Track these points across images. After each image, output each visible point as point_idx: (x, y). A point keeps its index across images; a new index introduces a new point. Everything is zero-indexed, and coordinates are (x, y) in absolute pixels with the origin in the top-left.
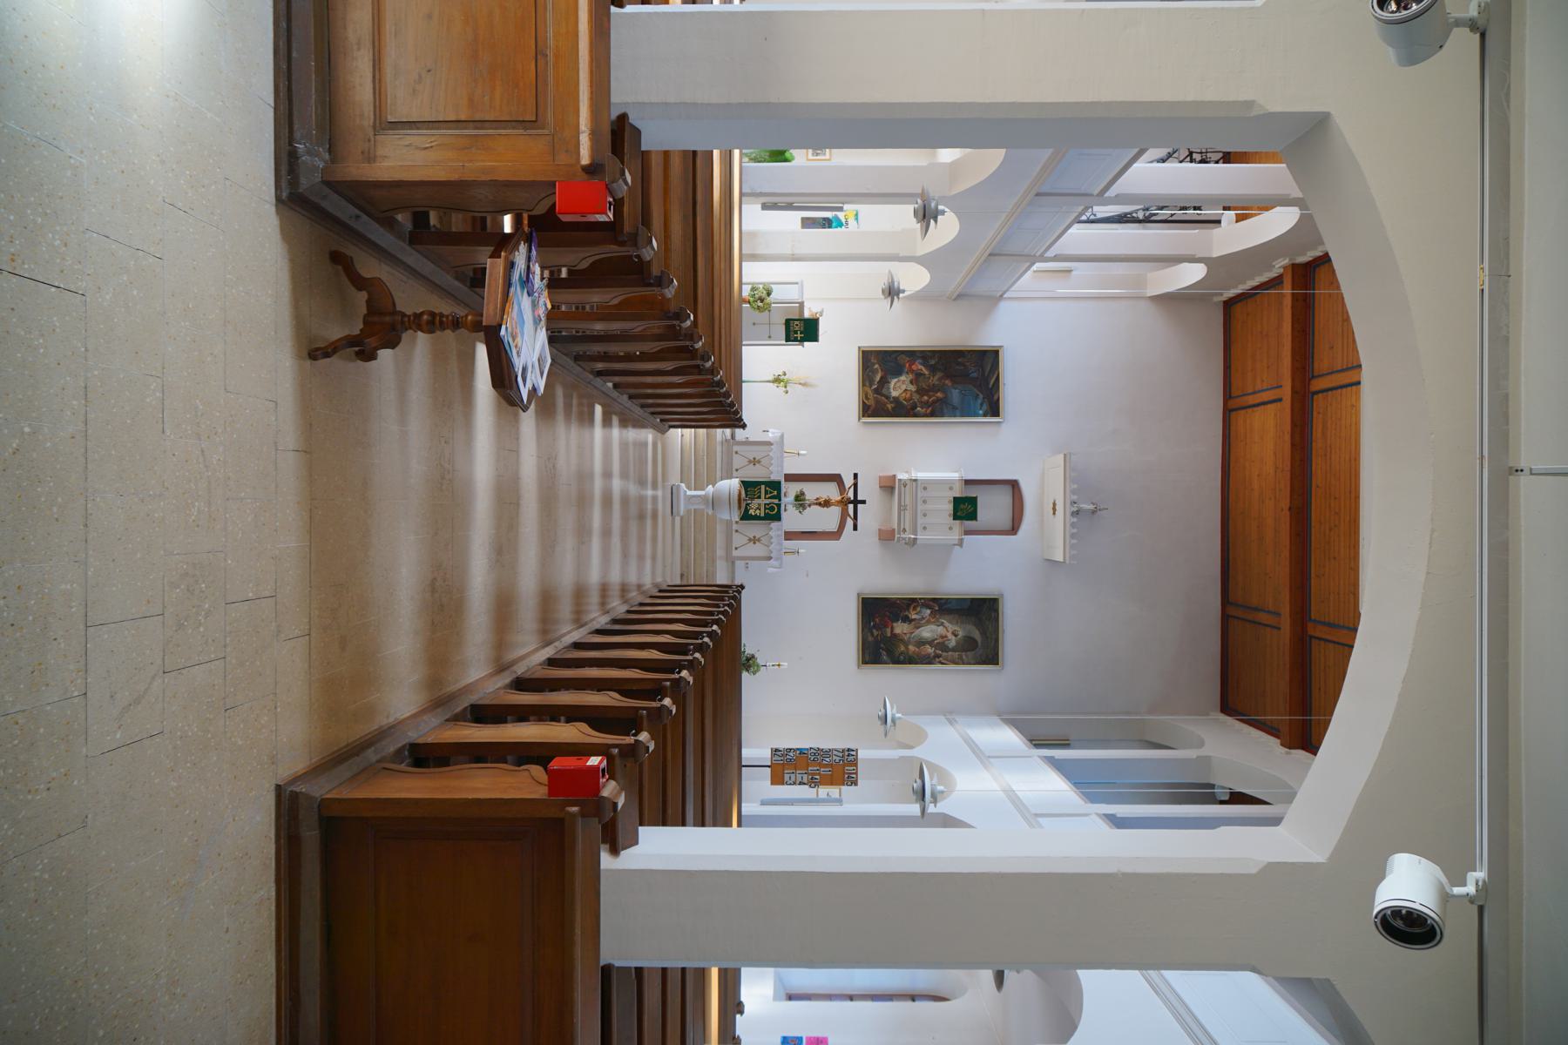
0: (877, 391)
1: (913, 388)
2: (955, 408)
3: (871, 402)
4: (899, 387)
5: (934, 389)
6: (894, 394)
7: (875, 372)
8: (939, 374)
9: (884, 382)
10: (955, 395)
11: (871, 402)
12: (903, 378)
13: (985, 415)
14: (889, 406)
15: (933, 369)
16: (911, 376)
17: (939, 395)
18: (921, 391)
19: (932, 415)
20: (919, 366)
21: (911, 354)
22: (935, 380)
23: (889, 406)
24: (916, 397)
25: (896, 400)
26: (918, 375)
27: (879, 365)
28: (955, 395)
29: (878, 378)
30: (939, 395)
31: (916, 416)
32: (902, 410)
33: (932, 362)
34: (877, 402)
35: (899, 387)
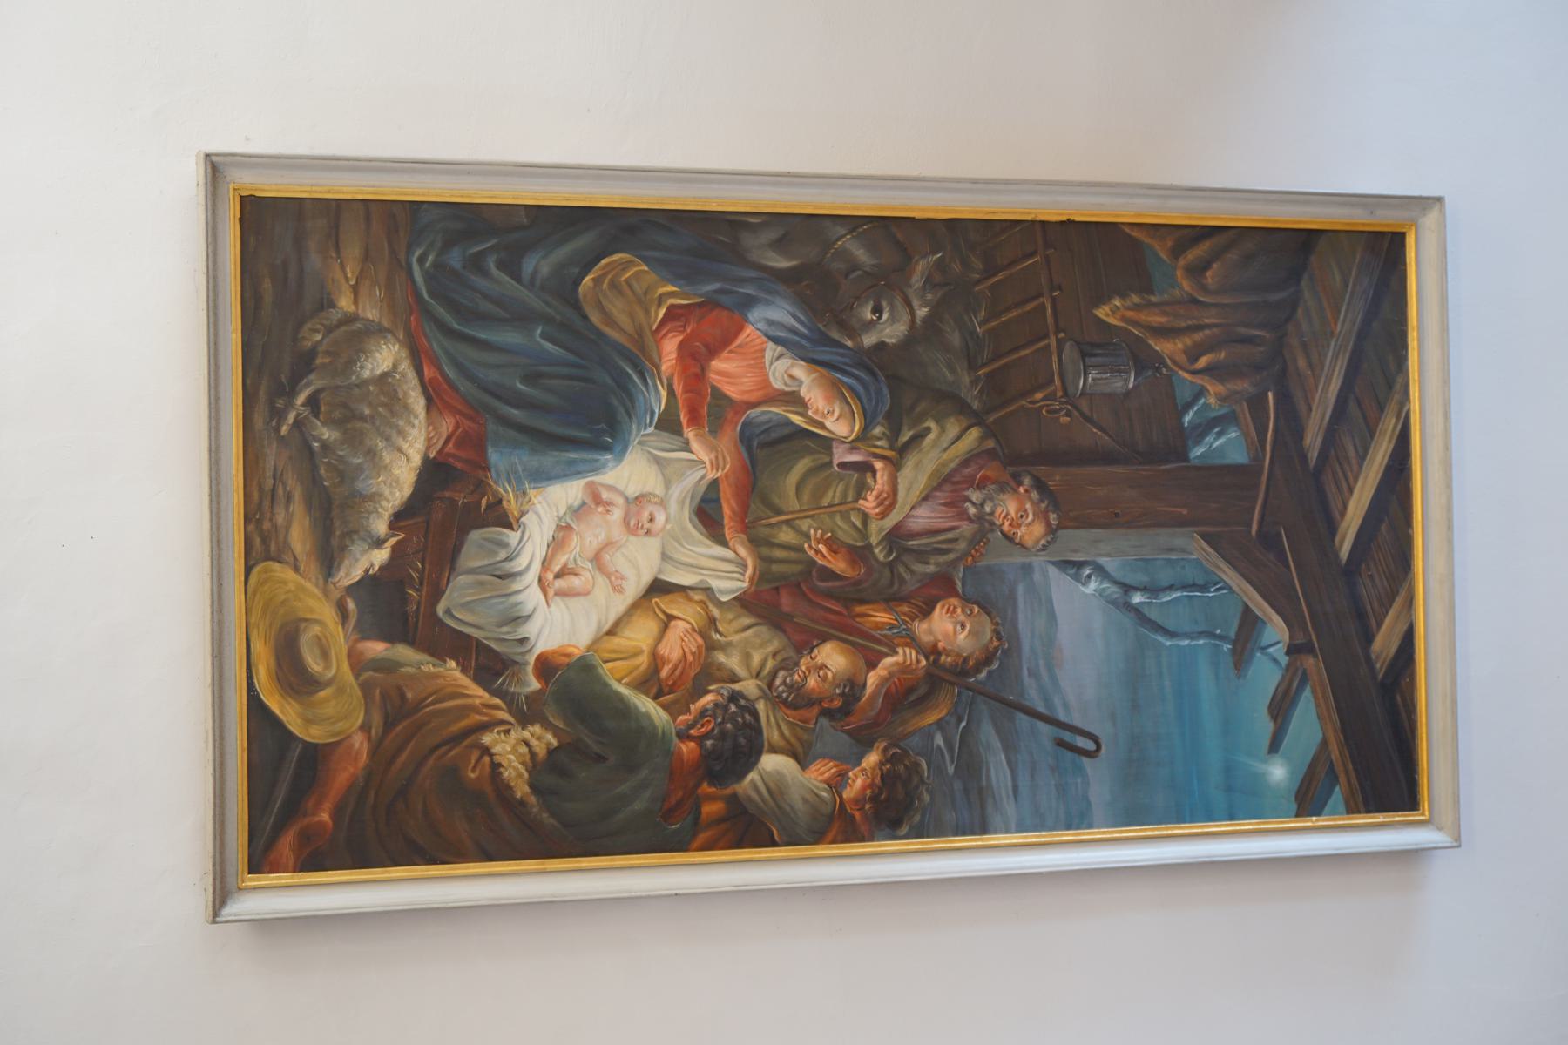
0: (395, 606)
1: (722, 569)
2: (1074, 744)
3: (334, 718)
4: (602, 560)
5: (903, 575)
6: (557, 626)
7: (364, 413)
8: (945, 443)
9: (454, 506)
10: (1077, 622)
11: (334, 718)
12: (631, 472)
13: (1308, 800)
14: (512, 750)
15: (894, 392)
16: (702, 460)
17: (949, 628)
18: (790, 600)
19: (892, 812)
20: (767, 364)
21: (707, 247)
22: (907, 493)
23: (512, 750)
24: (748, 652)
25: (572, 688)
26: (770, 445)
27: (396, 330)
28: (1077, 622)
29: (397, 473)
30: (949, 628)
31: (750, 829)
32: (629, 782)
33: (891, 330)
34: (396, 708)
35: (602, 560)
